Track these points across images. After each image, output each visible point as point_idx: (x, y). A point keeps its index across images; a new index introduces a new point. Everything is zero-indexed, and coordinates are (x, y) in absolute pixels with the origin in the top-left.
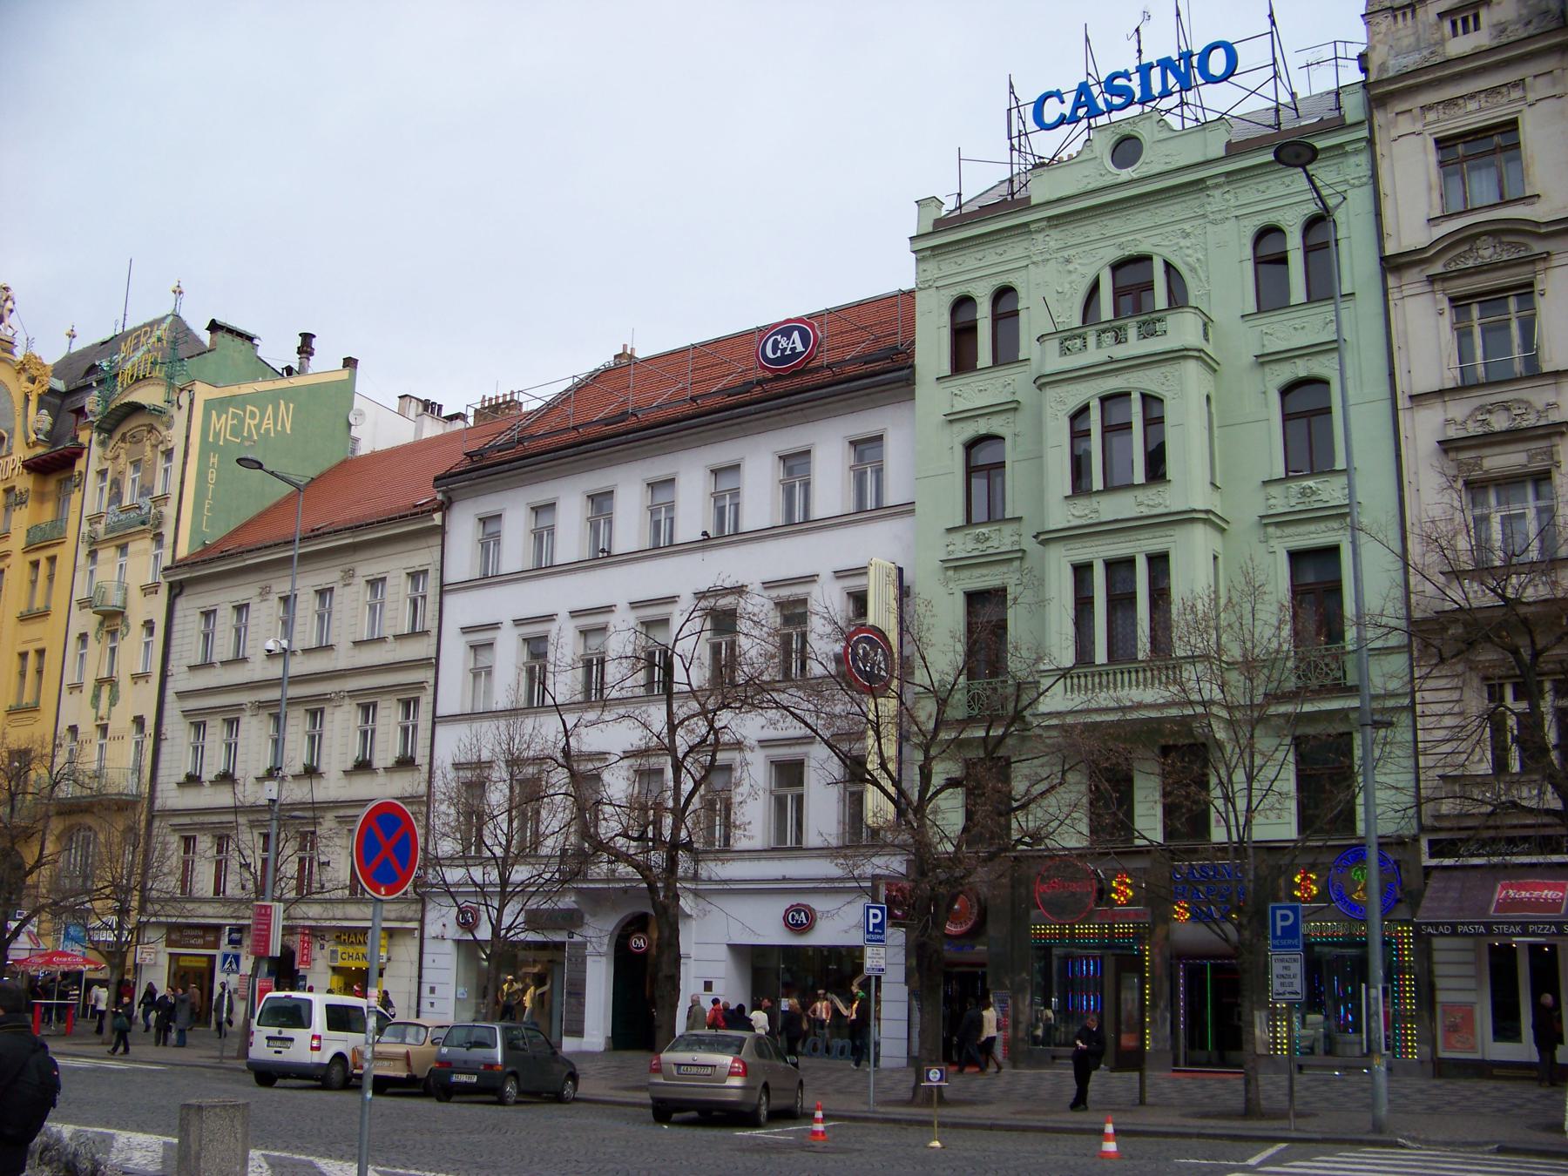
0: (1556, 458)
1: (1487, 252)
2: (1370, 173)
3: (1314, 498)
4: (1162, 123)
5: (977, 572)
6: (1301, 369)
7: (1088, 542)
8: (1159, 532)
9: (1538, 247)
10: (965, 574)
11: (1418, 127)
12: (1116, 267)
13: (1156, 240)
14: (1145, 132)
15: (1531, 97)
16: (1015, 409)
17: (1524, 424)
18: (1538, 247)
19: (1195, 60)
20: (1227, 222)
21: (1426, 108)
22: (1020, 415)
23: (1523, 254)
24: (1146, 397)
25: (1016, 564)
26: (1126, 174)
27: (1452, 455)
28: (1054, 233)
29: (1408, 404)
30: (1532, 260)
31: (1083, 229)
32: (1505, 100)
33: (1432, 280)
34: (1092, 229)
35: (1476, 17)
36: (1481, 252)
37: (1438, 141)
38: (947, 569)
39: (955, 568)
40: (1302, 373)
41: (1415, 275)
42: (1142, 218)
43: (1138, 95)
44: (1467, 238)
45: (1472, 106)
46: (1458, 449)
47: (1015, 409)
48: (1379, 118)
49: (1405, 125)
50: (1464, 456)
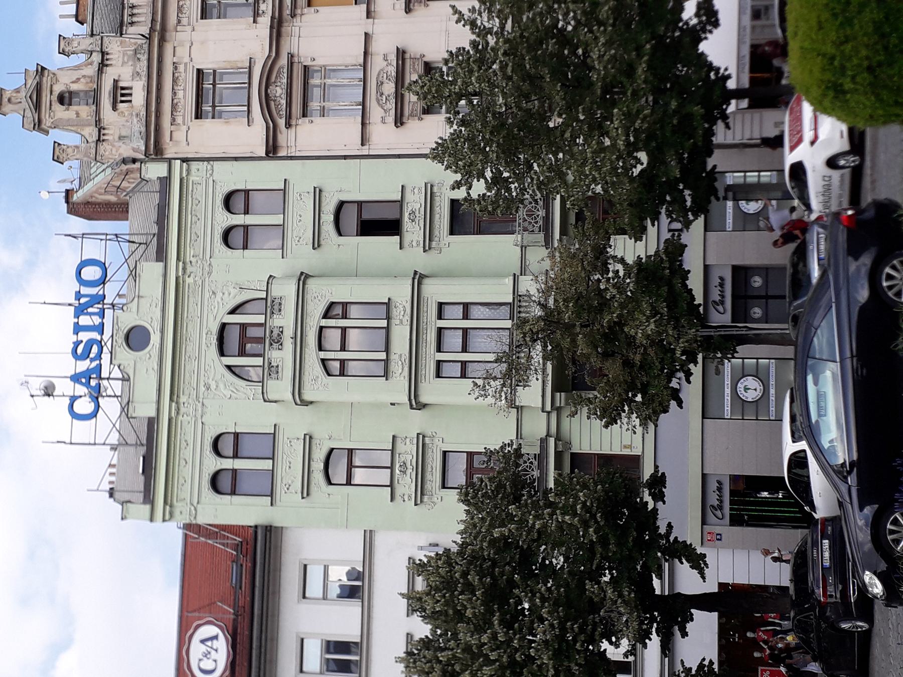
0: (418, 56)
1: (278, 91)
2: (205, 163)
3: (417, 212)
4: (125, 308)
5: (428, 476)
6: (328, 218)
7: (422, 362)
8: (423, 308)
9: (283, 61)
10: (428, 486)
11: (184, 128)
12: (222, 353)
13: (211, 318)
14: (128, 320)
15: (187, 60)
16: (311, 438)
17: (394, 74)
18: (283, 61)
19: (85, 290)
20: (212, 264)
21: (173, 121)
22: (315, 436)
23: (285, 70)
24: (326, 316)
25: (427, 440)
26: (155, 339)
27: (405, 120)
28: (183, 399)
29: (366, 147)
30: (291, 64)
31: (187, 375)
32: (183, 75)
33: (288, 125)
34: (188, 367)
35: (123, 88)
36: (278, 95)
37: (197, 117)
38: (421, 501)
39: (422, 494)
40: (331, 218)
41: (282, 139)
42: (191, 329)
43: (95, 335)
44: (267, 101)
45: (180, 94)
46: (402, 115)
47: (311, 438)
48: (168, 154)
49: (180, 135)
50: (407, 112)
